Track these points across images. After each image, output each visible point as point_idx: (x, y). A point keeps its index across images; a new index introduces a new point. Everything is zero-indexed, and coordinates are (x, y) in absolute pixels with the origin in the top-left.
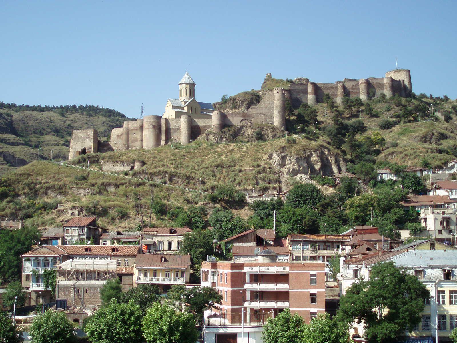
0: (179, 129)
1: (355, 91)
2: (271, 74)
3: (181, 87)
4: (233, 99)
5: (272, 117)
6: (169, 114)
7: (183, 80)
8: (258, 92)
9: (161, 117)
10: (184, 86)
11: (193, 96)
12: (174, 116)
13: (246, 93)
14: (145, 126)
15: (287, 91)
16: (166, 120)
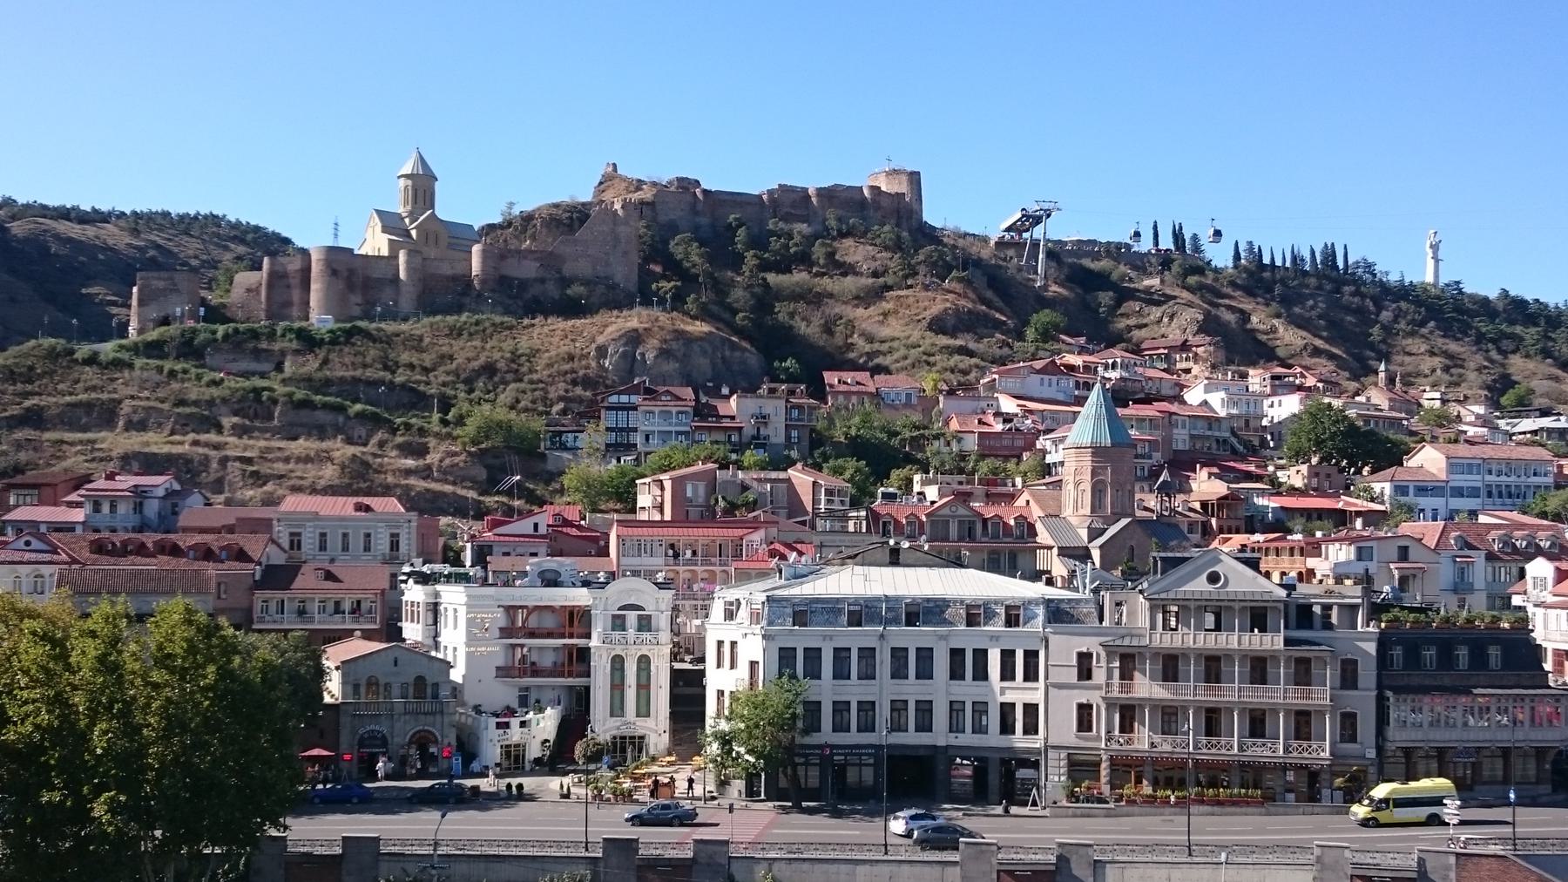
1: (798, 212)
2: (615, 165)
3: (402, 182)
4: (527, 218)
5: (608, 264)
6: (376, 243)
7: (407, 170)
8: (583, 204)
9: (351, 250)
10: (410, 182)
11: (432, 207)
12: (385, 252)
13: (556, 206)
14: (316, 268)
15: (648, 204)
16: (366, 257)
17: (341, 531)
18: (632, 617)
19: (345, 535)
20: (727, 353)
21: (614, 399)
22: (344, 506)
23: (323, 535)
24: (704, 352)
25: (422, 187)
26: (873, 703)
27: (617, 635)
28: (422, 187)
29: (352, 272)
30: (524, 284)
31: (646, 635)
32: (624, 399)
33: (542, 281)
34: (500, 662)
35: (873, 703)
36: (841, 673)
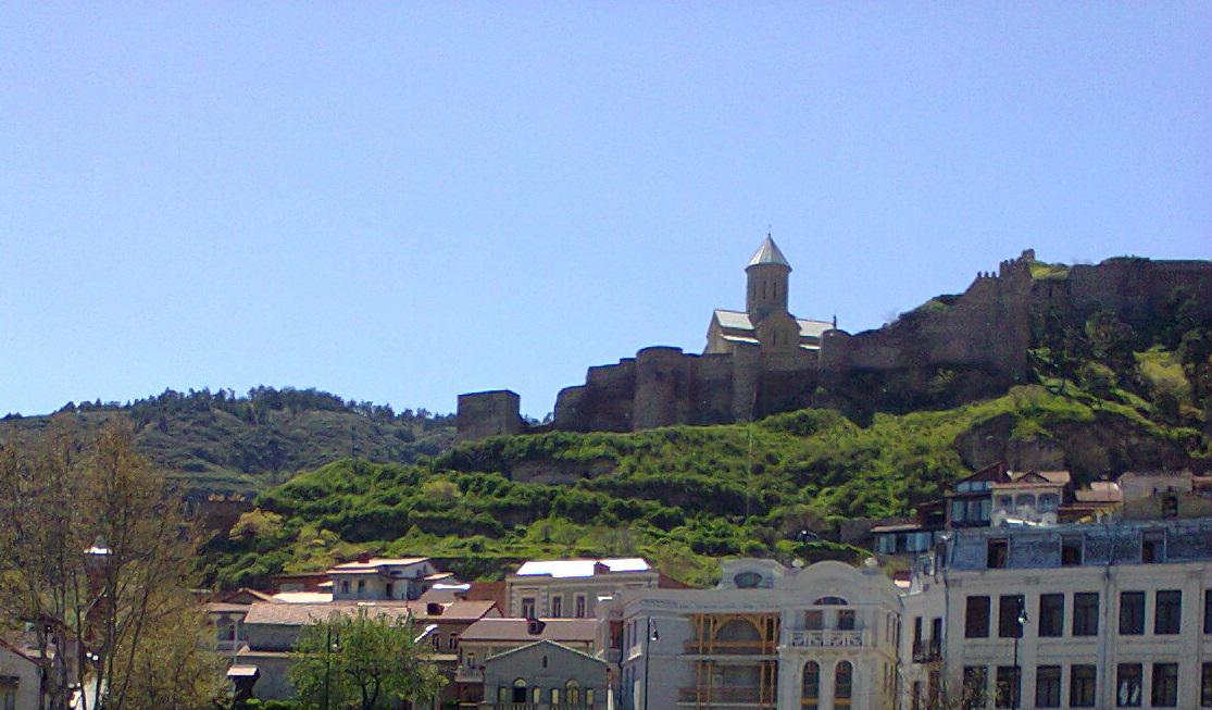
0: (728, 382)
17: (576, 595)
18: (830, 614)
19: (581, 599)
20: (1134, 441)
21: (964, 488)
22: (585, 568)
23: (557, 600)
24: (1101, 440)
25: (769, 284)
26: (1094, 668)
27: (808, 636)
28: (768, 283)
29: (677, 375)
30: (879, 375)
31: (846, 635)
32: (977, 486)
33: (903, 370)
34: (686, 683)
35: (1094, 668)
36: (1049, 627)
